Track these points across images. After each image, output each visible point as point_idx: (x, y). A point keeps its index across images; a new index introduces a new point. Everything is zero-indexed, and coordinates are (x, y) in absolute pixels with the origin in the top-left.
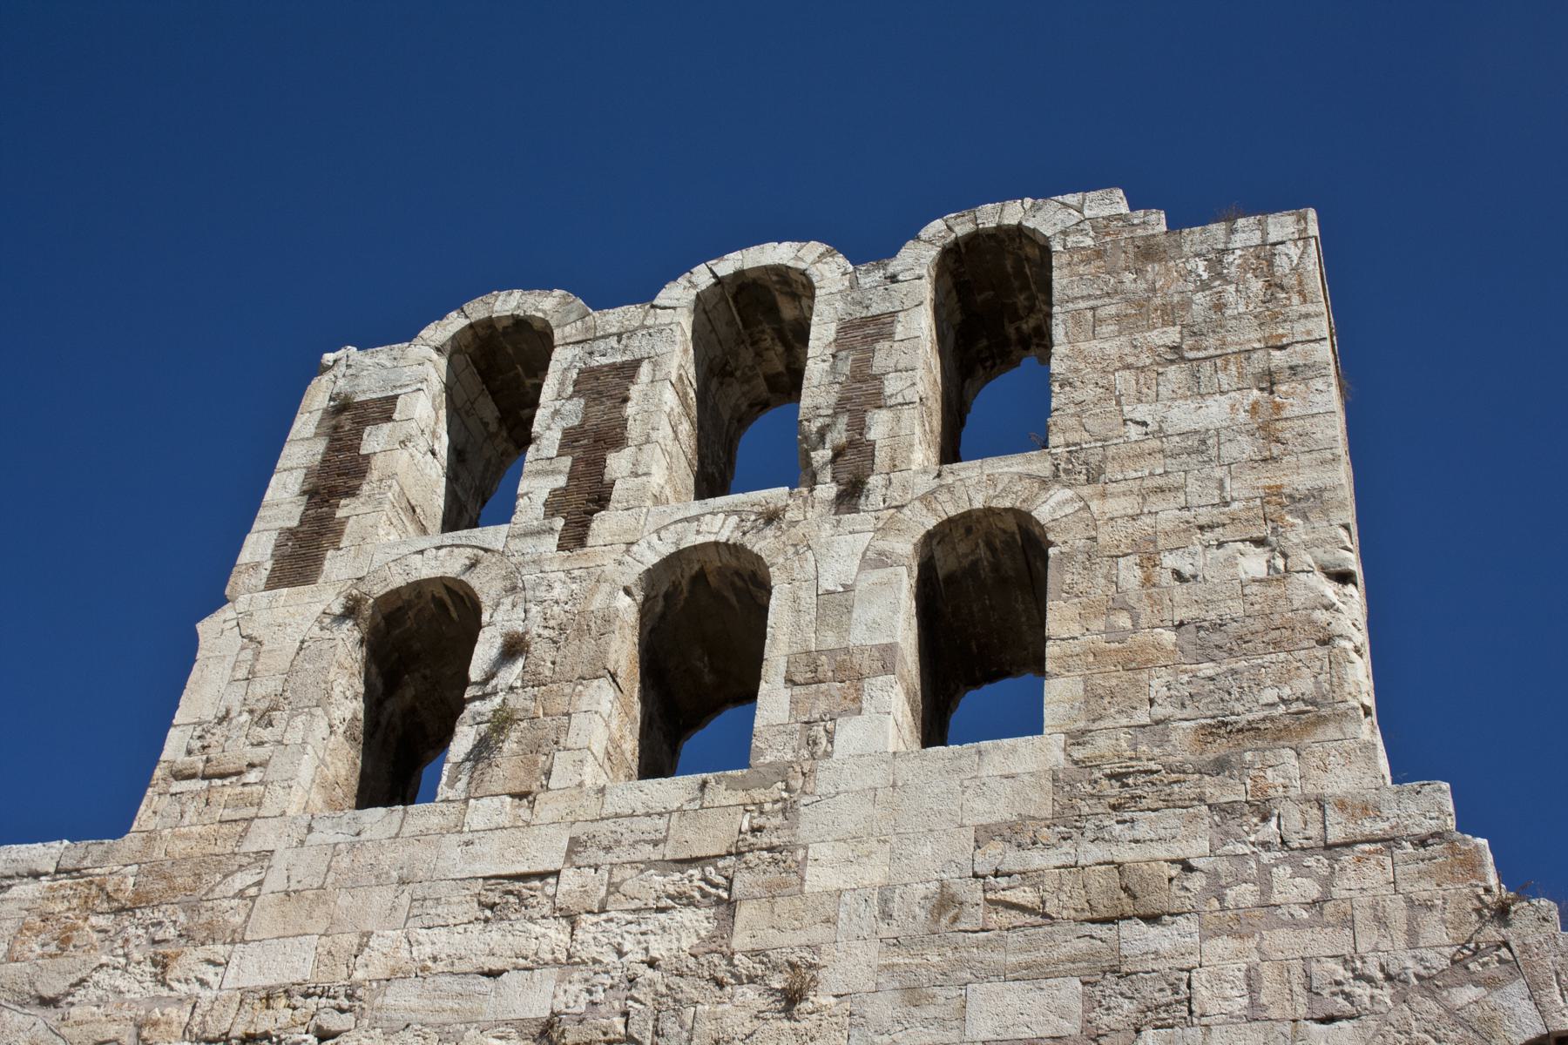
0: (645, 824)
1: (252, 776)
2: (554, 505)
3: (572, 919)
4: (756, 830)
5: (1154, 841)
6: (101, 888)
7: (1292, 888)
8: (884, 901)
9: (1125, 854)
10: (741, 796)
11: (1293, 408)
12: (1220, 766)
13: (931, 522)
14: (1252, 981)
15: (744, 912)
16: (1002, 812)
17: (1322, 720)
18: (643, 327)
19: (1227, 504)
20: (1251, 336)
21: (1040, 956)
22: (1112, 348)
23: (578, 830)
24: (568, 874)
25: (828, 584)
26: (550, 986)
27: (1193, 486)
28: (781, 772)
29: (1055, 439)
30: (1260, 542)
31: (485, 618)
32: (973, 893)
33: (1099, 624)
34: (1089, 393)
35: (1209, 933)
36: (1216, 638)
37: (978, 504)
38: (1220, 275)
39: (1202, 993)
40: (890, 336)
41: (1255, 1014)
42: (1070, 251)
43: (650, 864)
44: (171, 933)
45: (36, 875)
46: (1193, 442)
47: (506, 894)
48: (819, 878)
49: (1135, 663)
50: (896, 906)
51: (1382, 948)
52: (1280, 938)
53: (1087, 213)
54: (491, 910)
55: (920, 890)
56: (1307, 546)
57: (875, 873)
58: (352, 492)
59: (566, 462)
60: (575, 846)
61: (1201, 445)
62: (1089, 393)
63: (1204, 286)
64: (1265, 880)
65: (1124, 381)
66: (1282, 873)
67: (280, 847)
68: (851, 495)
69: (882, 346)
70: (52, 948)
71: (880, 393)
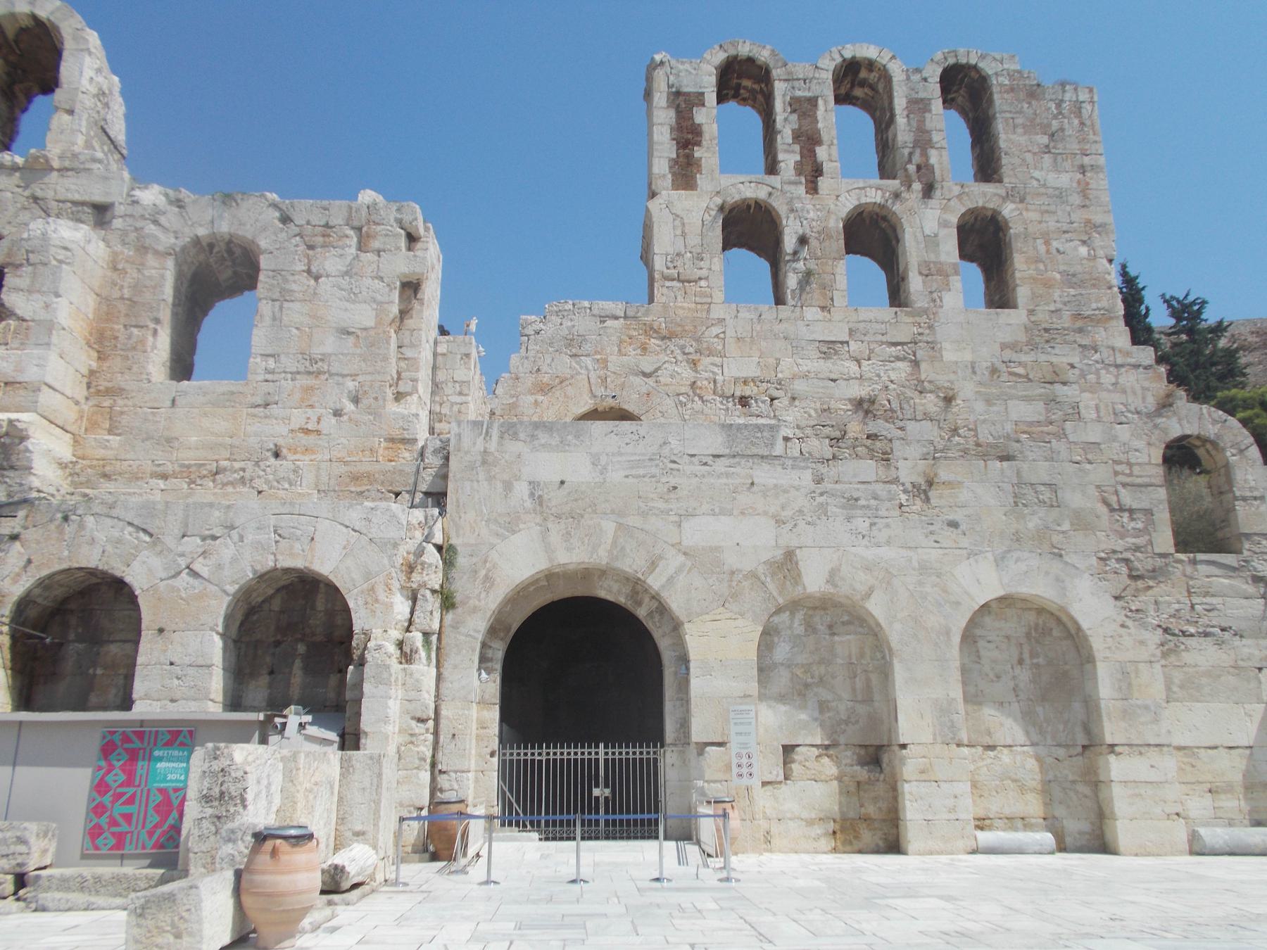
0: (878, 326)
1: (703, 283)
2: (799, 169)
3: (858, 361)
4: (920, 334)
5: (1063, 356)
6: (652, 328)
7: (1107, 378)
8: (973, 368)
9: (1054, 360)
10: (911, 320)
11: (1093, 185)
12: (1080, 330)
13: (963, 210)
14: (1097, 408)
15: (923, 366)
16: (1008, 339)
17: (1111, 318)
18: (814, 77)
19: (1072, 223)
20: (1074, 146)
21: (1029, 393)
22: (1023, 140)
23: (851, 325)
24: (851, 343)
25: (927, 232)
26: (857, 387)
27: (1060, 213)
28: (925, 311)
29: (1006, 180)
30: (1084, 242)
31: (784, 222)
32: (1003, 368)
33: (1033, 267)
34: (1017, 161)
35: (1083, 391)
36: (1074, 280)
37: (980, 204)
38: (1060, 113)
39: (1083, 411)
40: (930, 111)
41: (1099, 419)
42: (1001, 85)
43: (883, 343)
44: (692, 350)
45: (617, 318)
46: (1057, 192)
47: (829, 349)
48: (949, 355)
49: (1048, 284)
50: (977, 369)
51: (1135, 403)
52: (1104, 395)
53: (1006, 66)
54: (825, 355)
55: (985, 364)
56: (1102, 247)
57: (968, 356)
58: (699, 144)
59: (797, 148)
60: (851, 331)
61: (1060, 195)
62: (1017, 161)
63: (1055, 117)
64: (1097, 373)
65: (1029, 157)
66: (1103, 372)
67: (727, 317)
68: (928, 191)
69: (927, 115)
70: (639, 351)
71: (930, 140)
